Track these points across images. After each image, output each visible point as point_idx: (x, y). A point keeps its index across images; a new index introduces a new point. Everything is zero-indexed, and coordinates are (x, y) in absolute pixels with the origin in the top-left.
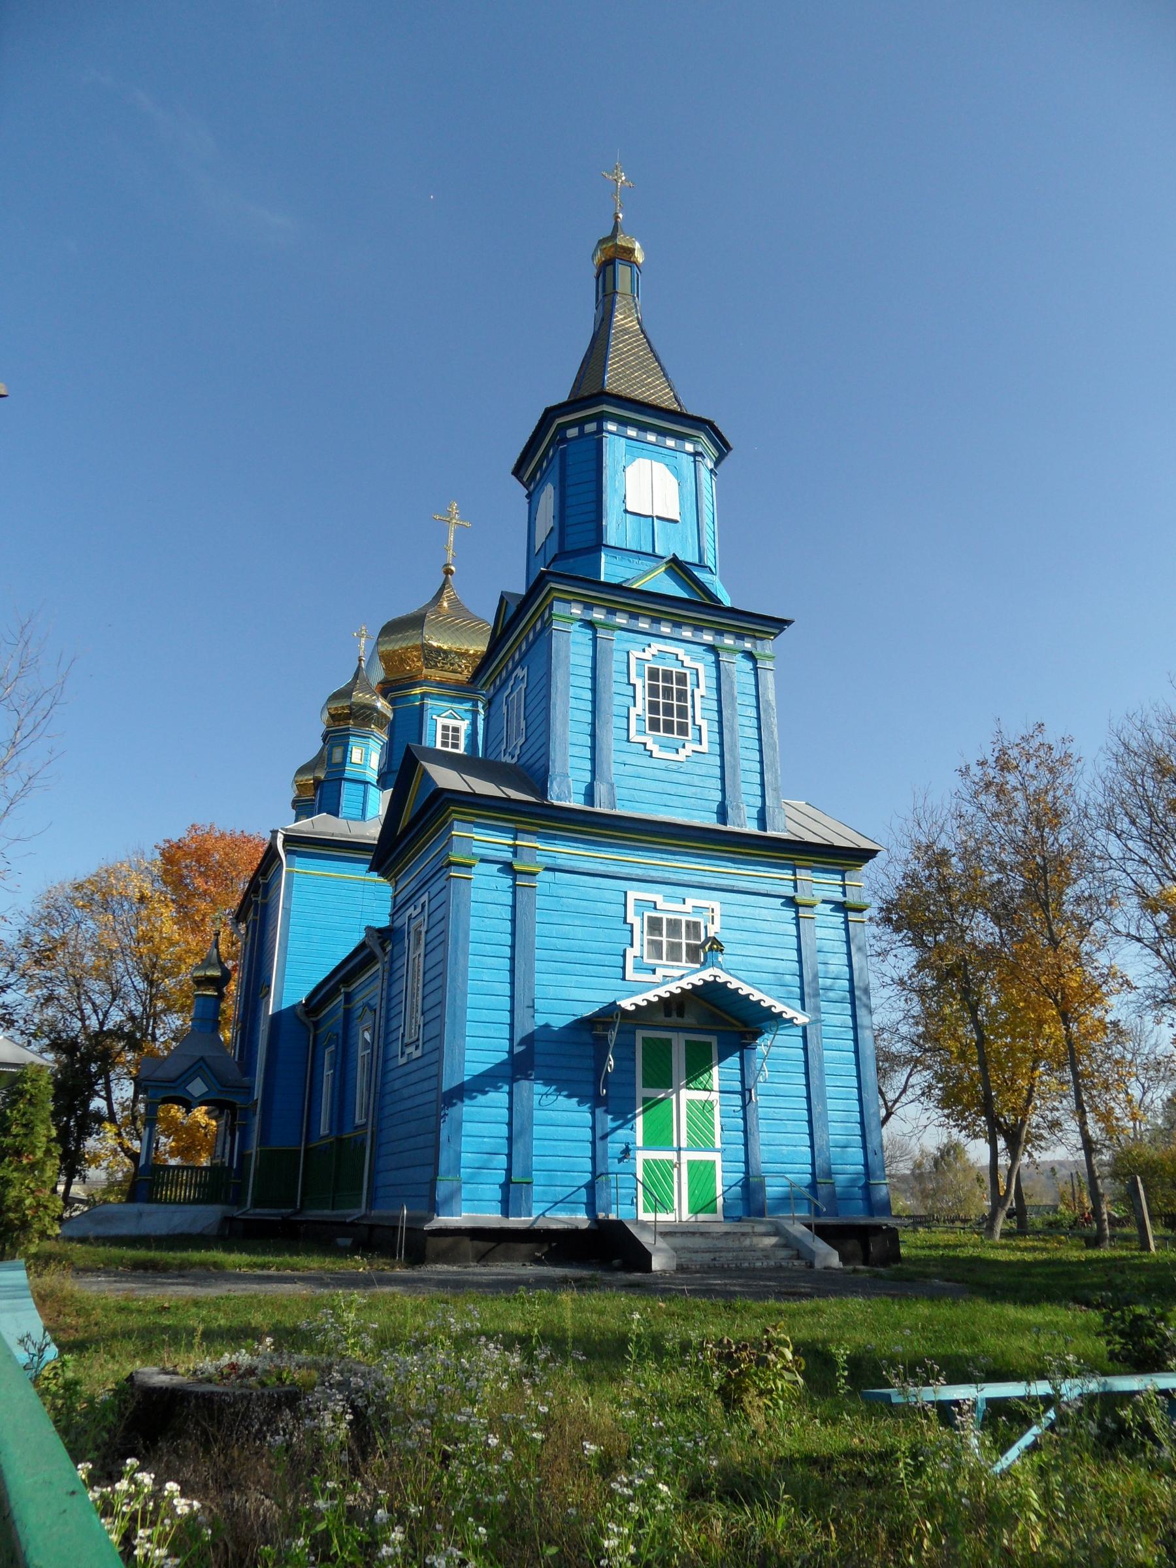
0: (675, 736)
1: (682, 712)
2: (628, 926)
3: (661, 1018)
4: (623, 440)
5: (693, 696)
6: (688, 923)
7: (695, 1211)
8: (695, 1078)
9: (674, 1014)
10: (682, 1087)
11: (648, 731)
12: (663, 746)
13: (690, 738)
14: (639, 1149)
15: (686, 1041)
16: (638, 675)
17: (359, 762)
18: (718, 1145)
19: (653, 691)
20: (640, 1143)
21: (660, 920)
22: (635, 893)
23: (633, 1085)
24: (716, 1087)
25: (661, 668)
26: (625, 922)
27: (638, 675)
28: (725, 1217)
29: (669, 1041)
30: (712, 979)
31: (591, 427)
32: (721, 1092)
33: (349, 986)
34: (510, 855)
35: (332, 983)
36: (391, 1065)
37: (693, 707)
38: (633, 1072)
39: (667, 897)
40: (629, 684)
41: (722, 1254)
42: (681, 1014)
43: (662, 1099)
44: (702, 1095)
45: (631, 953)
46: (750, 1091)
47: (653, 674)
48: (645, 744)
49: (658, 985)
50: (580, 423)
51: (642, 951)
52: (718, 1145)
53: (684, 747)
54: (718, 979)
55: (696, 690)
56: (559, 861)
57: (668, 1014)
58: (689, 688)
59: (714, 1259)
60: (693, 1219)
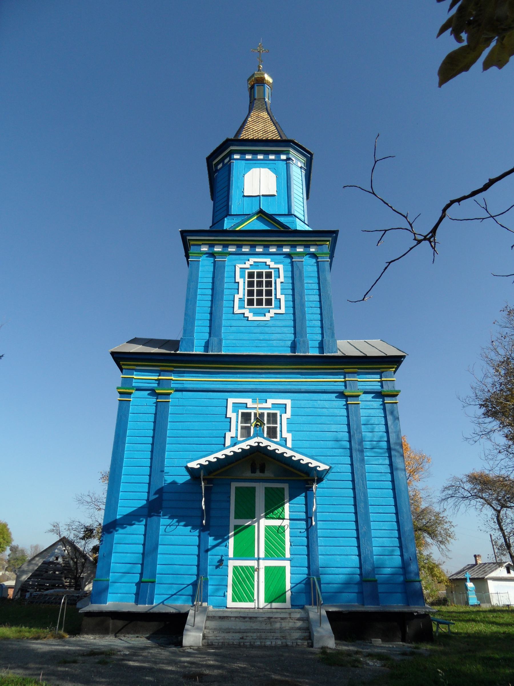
0: (255, 306)
1: (269, 293)
3: (248, 474)
4: (243, 162)
5: (275, 283)
6: (269, 414)
7: (270, 600)
8: (272, 512)
9: (258, 471)
10: (262, 517)
11: (246, 306)
12: (255, 314)
13: (273, 306)
14: (231, 559)
15: (266, 488)
16: (241, 277)
18: (288, 555)
19: (251, 284)
20: (231, 554)
21: (249, 414)
23: (228, 517)
24: (287, 516)
26: (226, 417)
27: (241, 277)
28: (292, 605)
29: (254, 488)
30: (256, 444)
32: (290, 519)
34: (156, 385)
37: (276, 289)
38: (229, 509)
40: (235, 282)
41: (249, 634)
42: (262, 471)
43: (248, 526)
44: (277, 523)
45: (229, 435)
46: (311, 518)
48: (244, 314)
51: (237, 433)
52: (288, 555)
53: (269, 312)
54: (261, 444)
55: (278, 280)
56: (185, 386)
57: (253, 471)
58: (273, 280)
59: (242, 638)
60: (269, 606)
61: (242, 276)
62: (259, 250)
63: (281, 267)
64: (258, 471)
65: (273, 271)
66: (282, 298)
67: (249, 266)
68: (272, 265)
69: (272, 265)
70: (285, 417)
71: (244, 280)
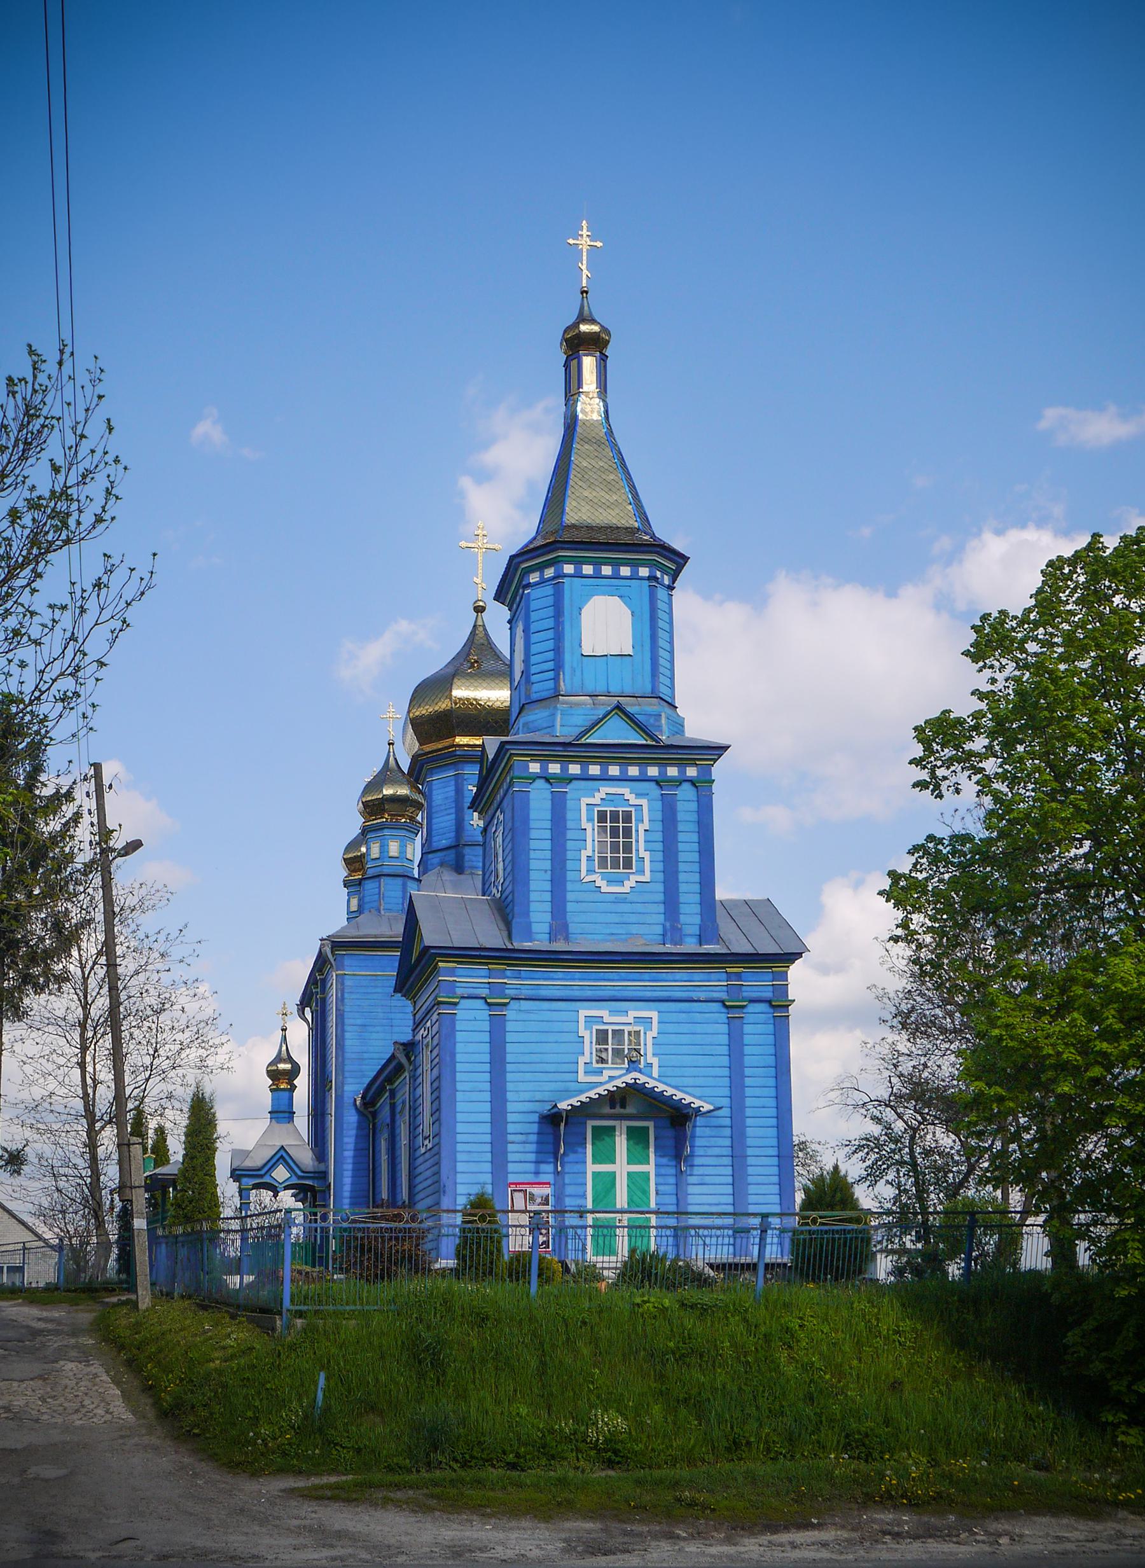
1: (628, 848)
2: (581, 1039)
3: (607, 1110)
5: (637, 831)
9: (618, 1106)
12: (610, 882)
17: (396, 855)
22: (583, 1013)
25: (608, 809)
31: (549, 572)
33: (392, 1084)
35: (378, 1082)
36: (418, 1154)
37: (637, 841)
39: (612, 1012)
42: (623, 1106)
45: (582, 1060)
47: (602, 817)
49: (601, 1084)
50: (541, 567)
51: (591, 1058)
55: (640, 826)
57: (613, 1107)
61: (590, 820)
62: (614, 771)
63: (644, 802)
64: (618, 1106)
65: (632, 809)
66: (646, 856)
67: (599, 802)
68: (633, 800)
69: (633, 800)
70: (650, 1035)
71: (593, 825)
